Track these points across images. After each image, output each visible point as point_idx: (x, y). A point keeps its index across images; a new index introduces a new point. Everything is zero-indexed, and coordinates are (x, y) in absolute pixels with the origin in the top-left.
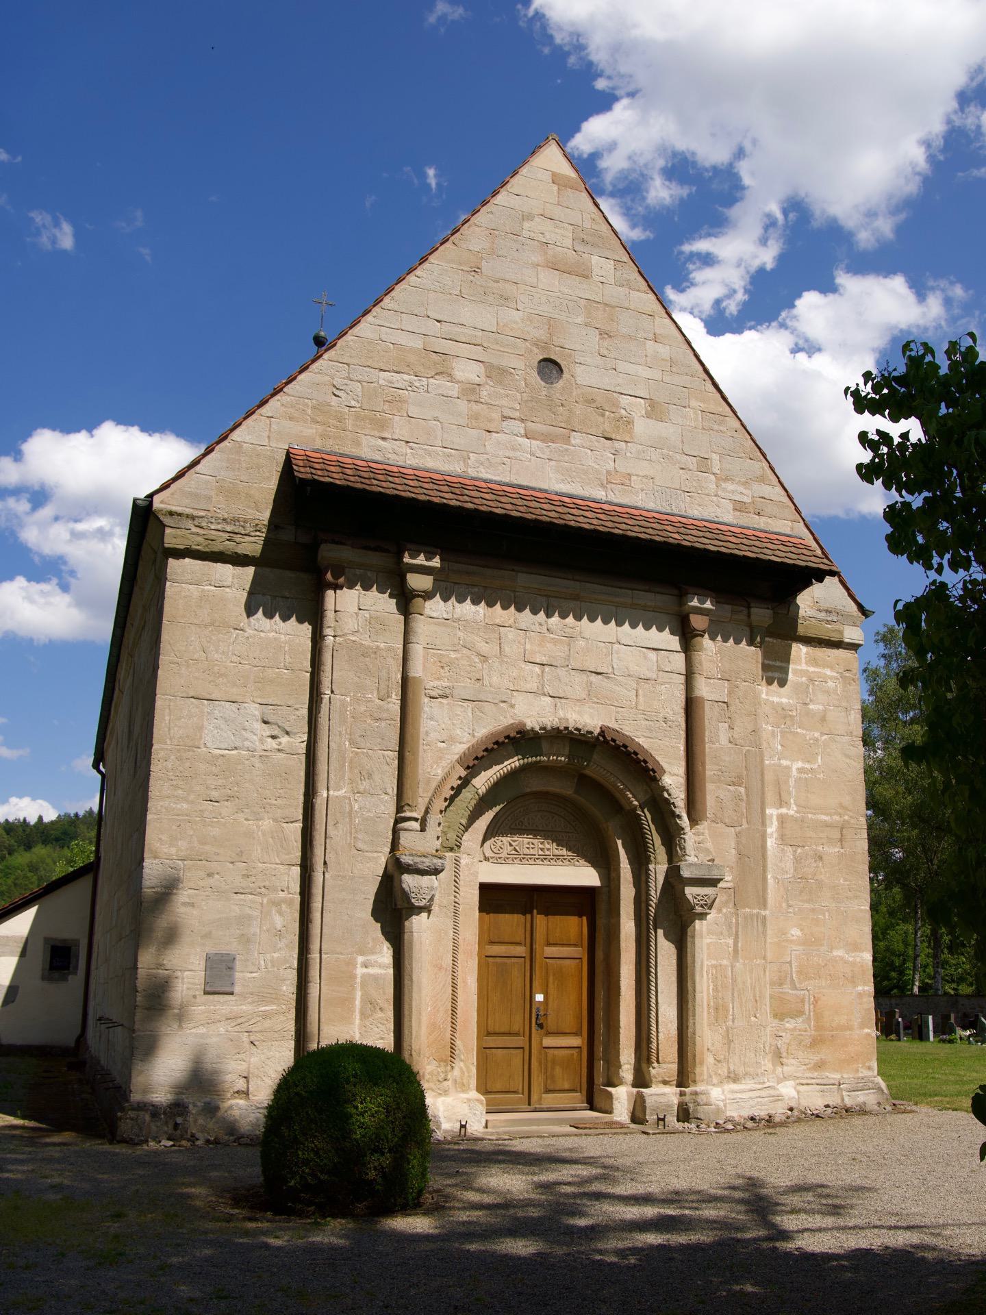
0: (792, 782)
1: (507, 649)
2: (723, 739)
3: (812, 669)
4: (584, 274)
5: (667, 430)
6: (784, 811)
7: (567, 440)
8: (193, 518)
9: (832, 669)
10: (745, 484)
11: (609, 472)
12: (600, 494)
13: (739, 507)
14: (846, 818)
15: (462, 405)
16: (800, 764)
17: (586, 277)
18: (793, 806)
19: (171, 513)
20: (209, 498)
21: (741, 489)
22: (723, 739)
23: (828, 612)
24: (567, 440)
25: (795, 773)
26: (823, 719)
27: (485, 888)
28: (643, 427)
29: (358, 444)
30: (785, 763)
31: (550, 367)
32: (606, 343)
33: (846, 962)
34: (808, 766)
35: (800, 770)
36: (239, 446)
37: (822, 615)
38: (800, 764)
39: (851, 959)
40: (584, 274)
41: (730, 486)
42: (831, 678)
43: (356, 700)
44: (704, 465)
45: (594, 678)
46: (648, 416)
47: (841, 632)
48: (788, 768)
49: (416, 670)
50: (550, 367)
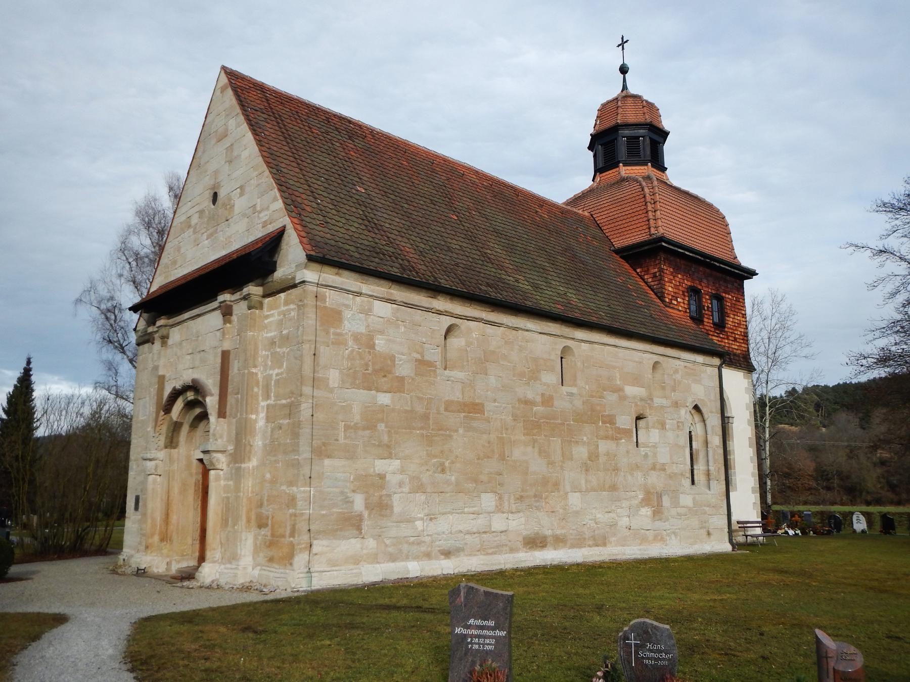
0: (273, 383)
2: (236, 371)
3: (286, 308)
6: (269, 402)
9: (293, 303)
14: (293, 399)
16: (276, 371)
18: (273, 398)
22: (236, 371)
25: (274, 377)
26: (288, 338)
30: (271, 372)
31: (215, 197)
33: (286, 493)
34: (280, 371)
35: (277, 375)
38: (276, 371)
39: (288, 492)
42: (293, 310)
47: (294, 278)
48: (272, 374)
50: (215, 197)
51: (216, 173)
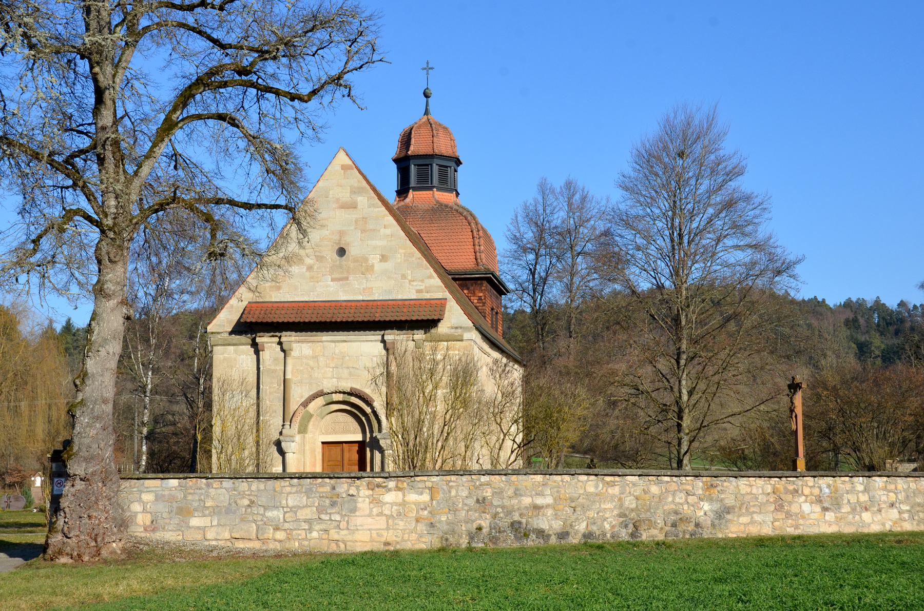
1: (320, 364)
4: (353, 206)
5: (388, 265)
7: (347, 279)
8: (218, 333)
10: (422, 281)
11: (364, 289)
12: (360, 298)
13: (419, 291)
15: (308, 274)
17: (356, 208)
19: (212, 333)
20: (224, 326)
21: (420, 283)
23: (456, 328)
24: (347, 279)
27: (323, 443)
28: (378, 266)
29: (271, 297)
31: (342, 252)
32: (363, 235)
36: (232, 306)
37: (453, 330)
40: (353, 206)
41: (415, 283)
43: (270, 387)
44: (404, 277)
45: (351, 370)
46: (381, 261)
47: (462, 336)
49: (288, 376)
50: (342, 252)
51: (342, 233)
